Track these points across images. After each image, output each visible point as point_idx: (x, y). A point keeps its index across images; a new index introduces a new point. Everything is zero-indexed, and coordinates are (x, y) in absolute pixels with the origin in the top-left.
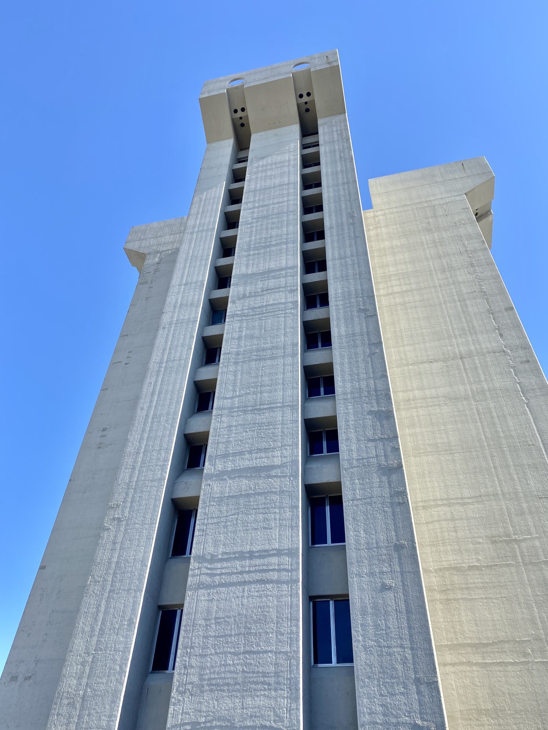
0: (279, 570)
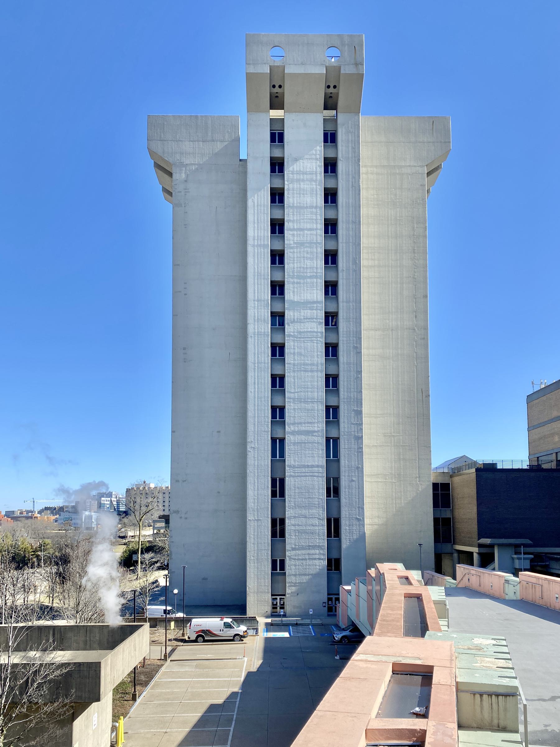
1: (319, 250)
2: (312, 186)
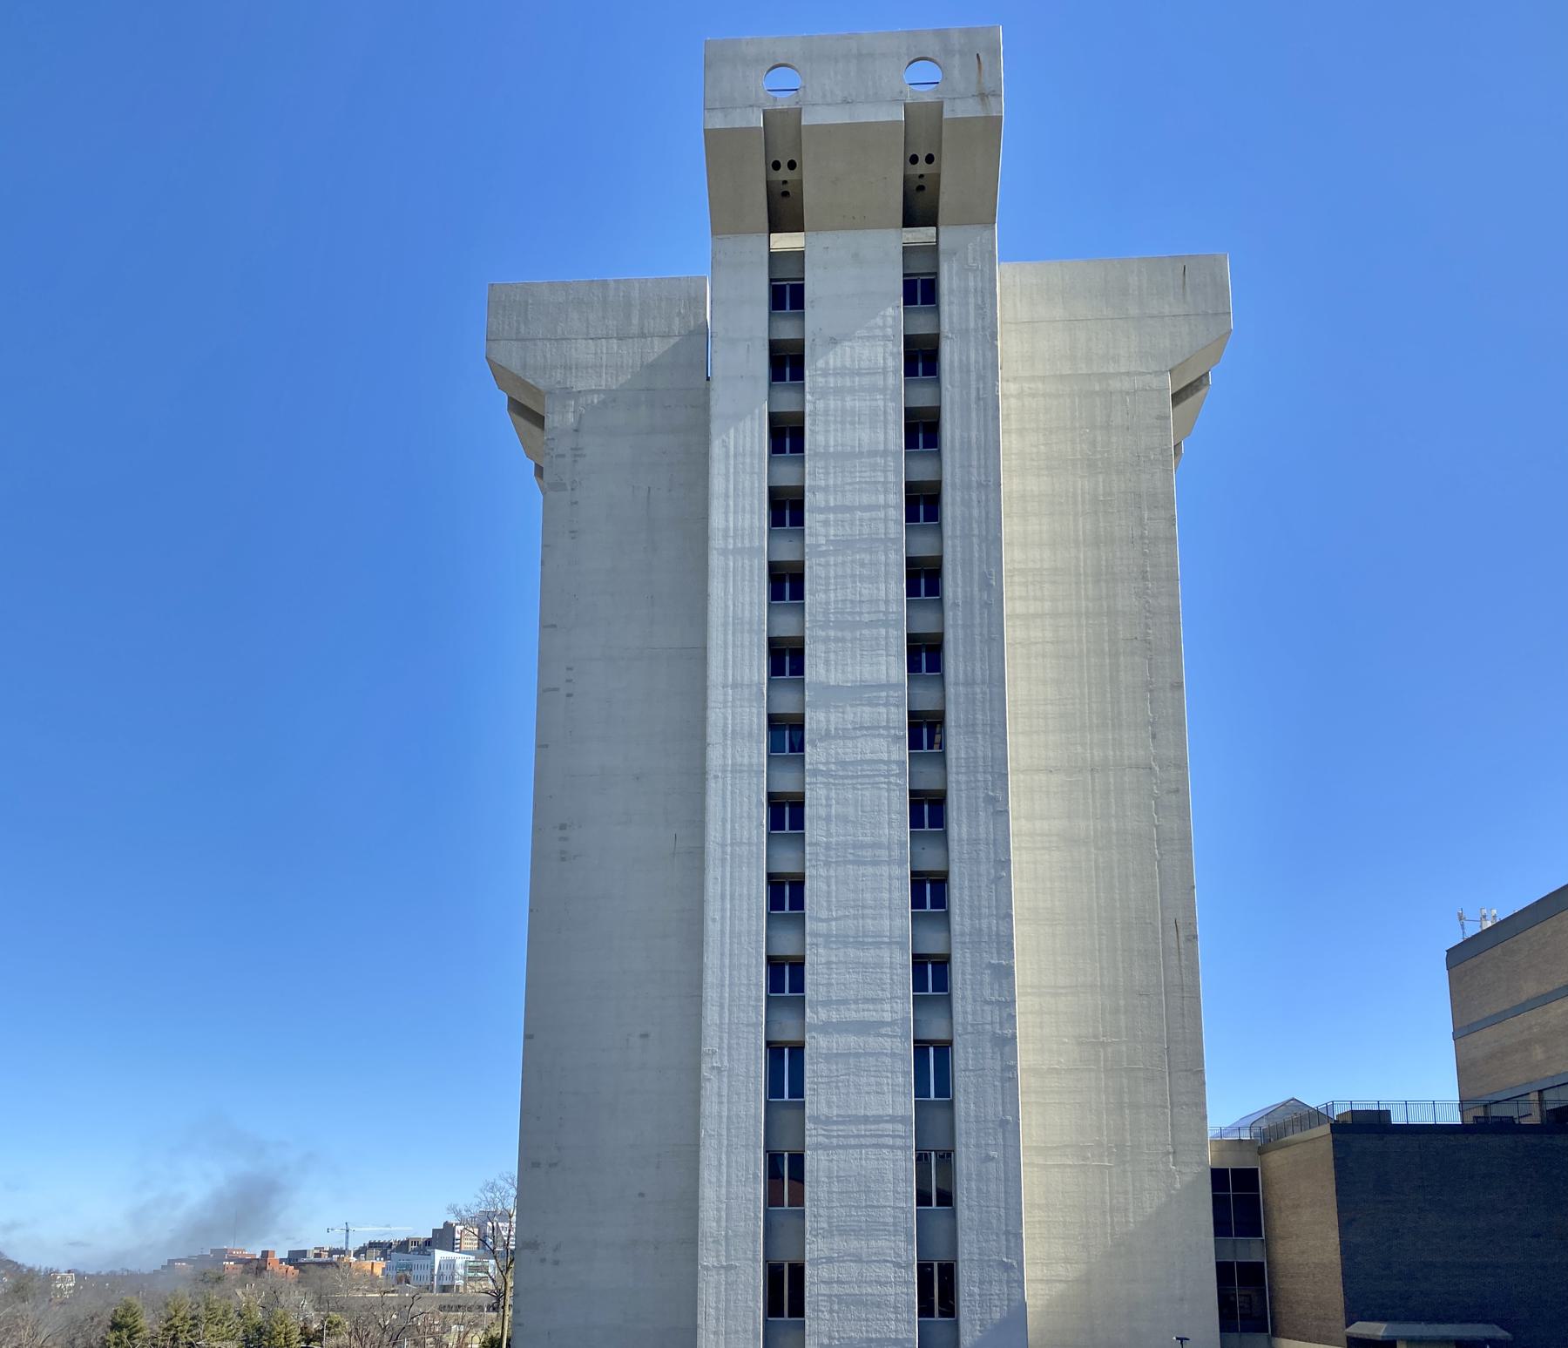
0: (894, 1137)
1: (892, 556)
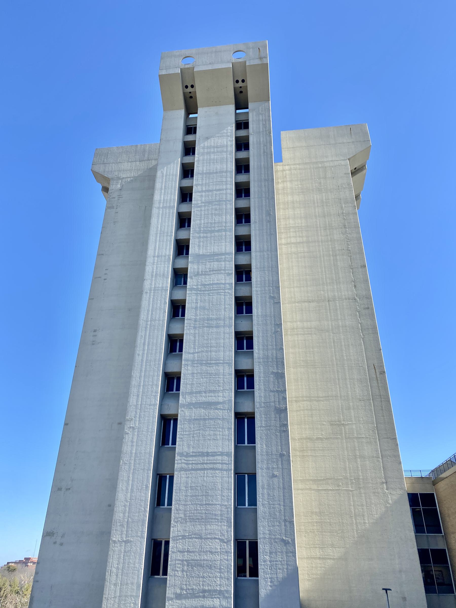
0: (222, 464)
2: (222, 156)
